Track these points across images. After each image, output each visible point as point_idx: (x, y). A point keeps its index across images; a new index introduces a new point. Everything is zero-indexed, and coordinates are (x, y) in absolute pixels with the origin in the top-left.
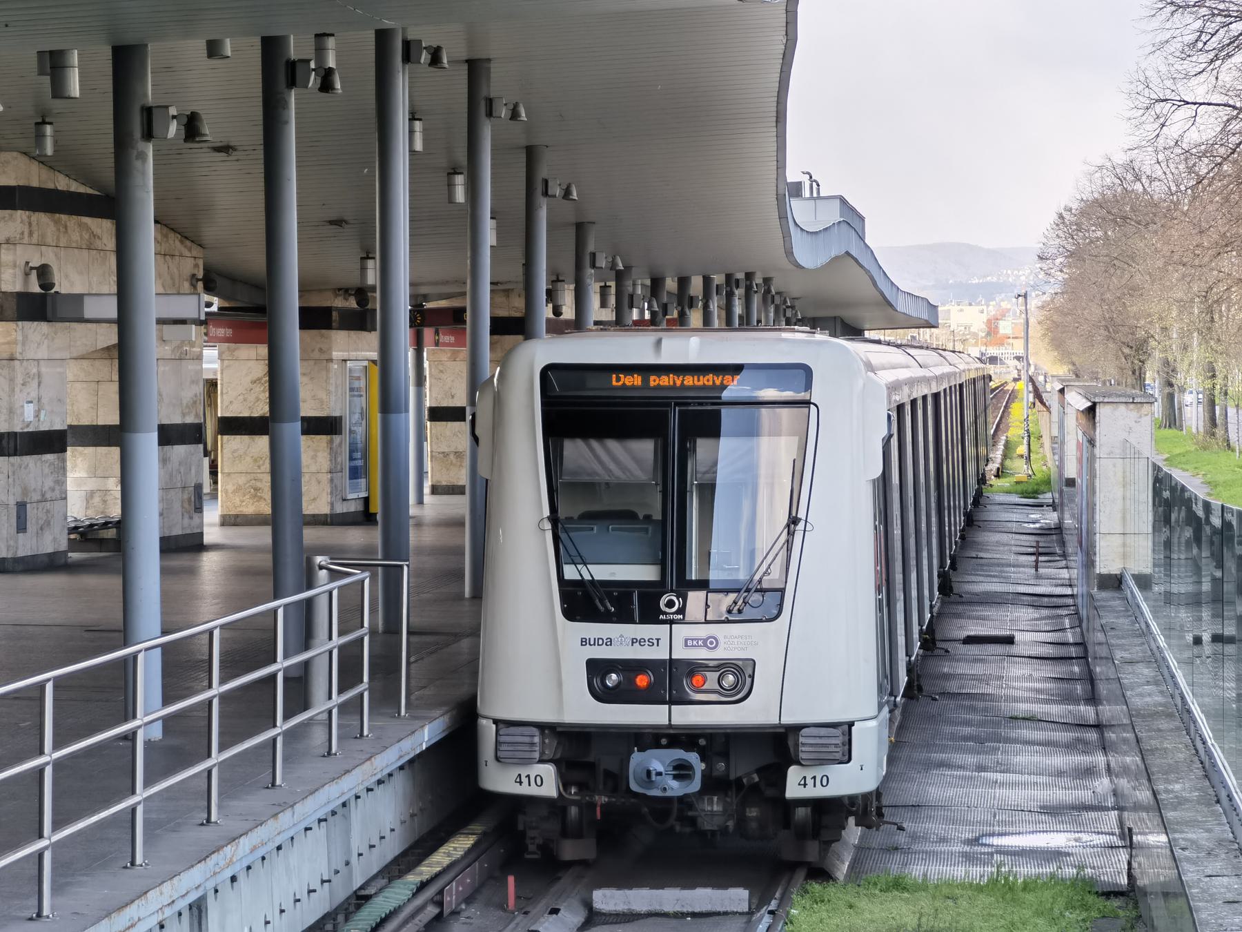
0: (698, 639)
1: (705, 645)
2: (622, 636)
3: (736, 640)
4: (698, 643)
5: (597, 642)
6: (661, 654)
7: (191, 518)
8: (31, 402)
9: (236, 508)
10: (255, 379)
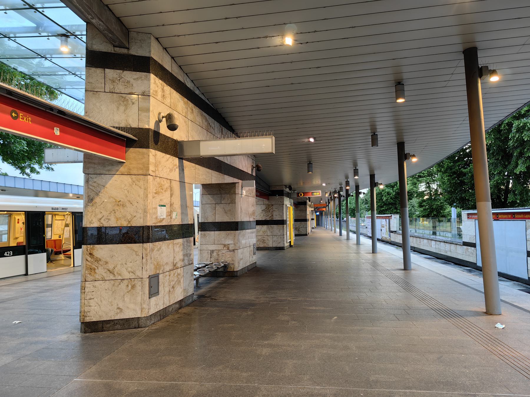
7: (252, 257)
8: (165, 206)
10: (263, 209)
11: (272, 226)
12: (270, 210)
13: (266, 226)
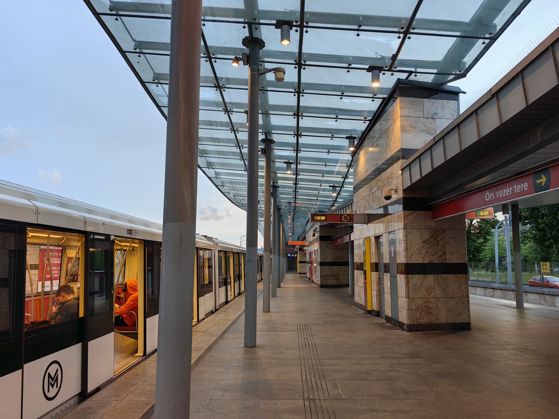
9: (417, 320)
11: (444, 276)
12: (438, 241)
13: (432, 275)
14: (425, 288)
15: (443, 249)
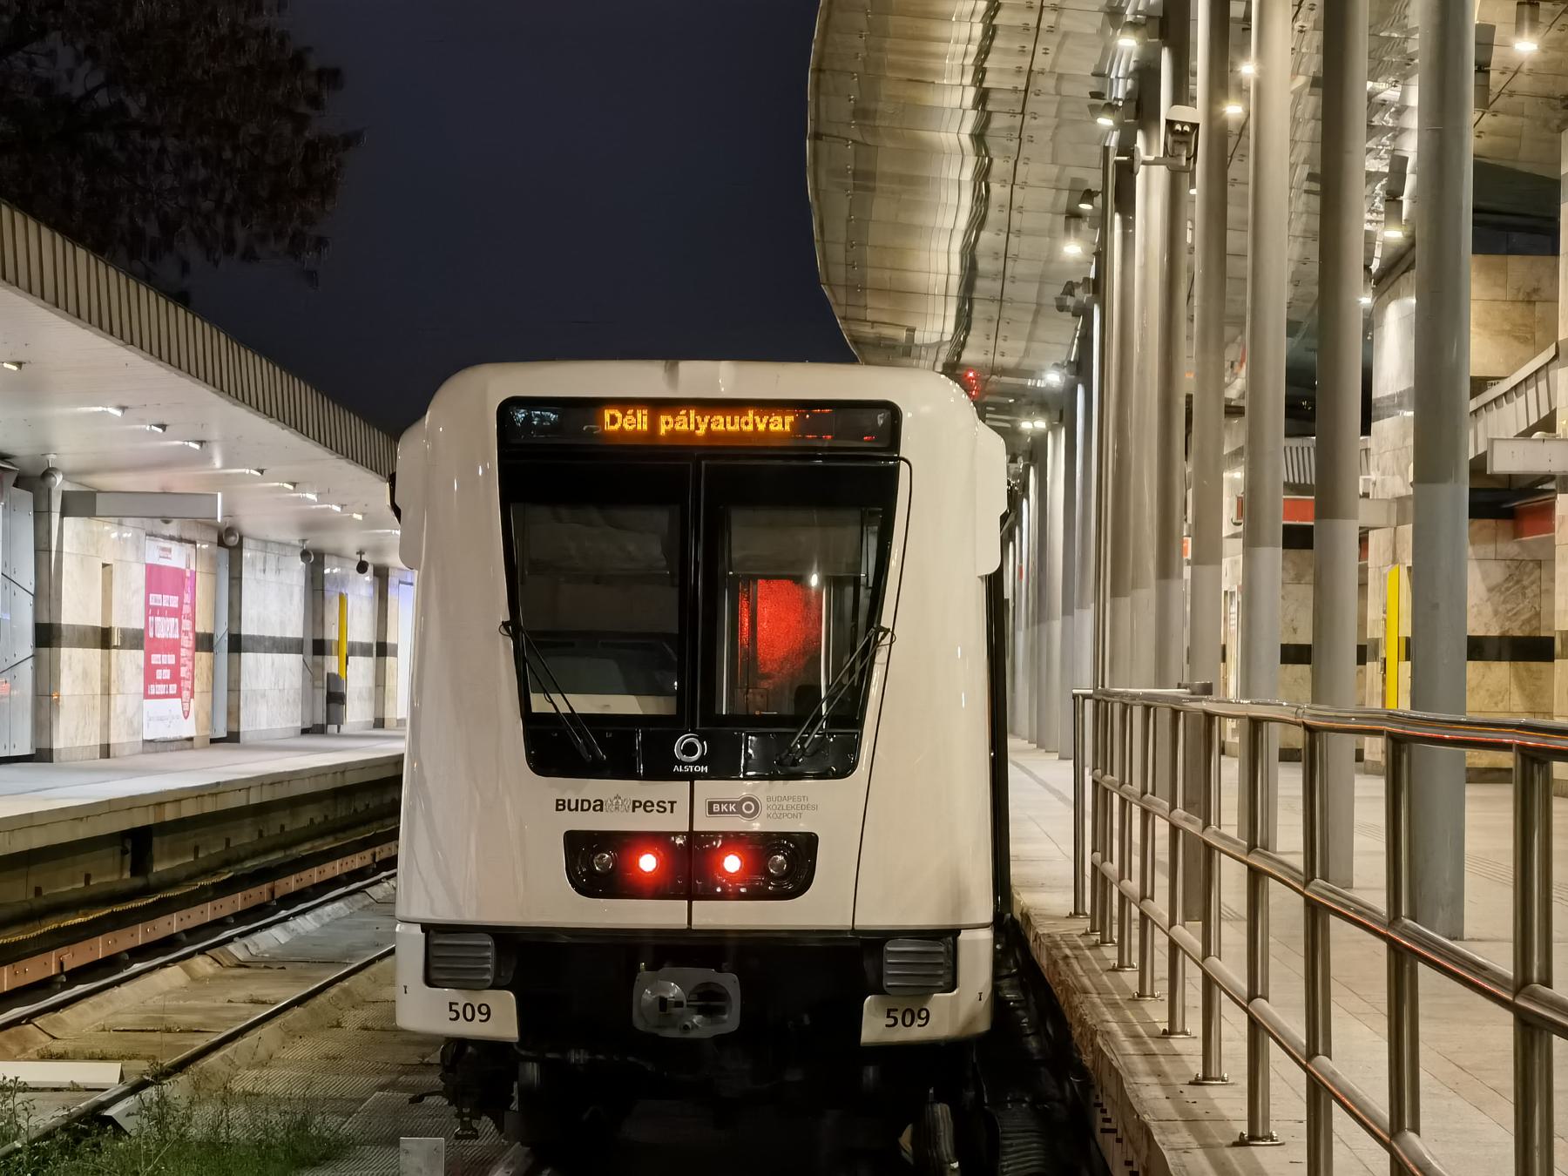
0: (728, 803)
1: (739, 811)
2: (618, 797)
3: (785, 803)
4: (728, 808)
5: (581, 806)
6: (675, 822)
10: (1494, 583)
12: (1524, 588)
14: (1488, 690)
15: (1537, 606)
